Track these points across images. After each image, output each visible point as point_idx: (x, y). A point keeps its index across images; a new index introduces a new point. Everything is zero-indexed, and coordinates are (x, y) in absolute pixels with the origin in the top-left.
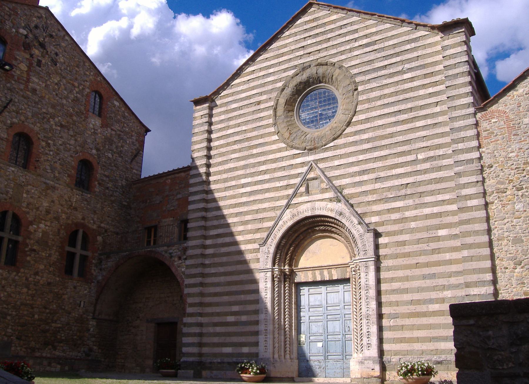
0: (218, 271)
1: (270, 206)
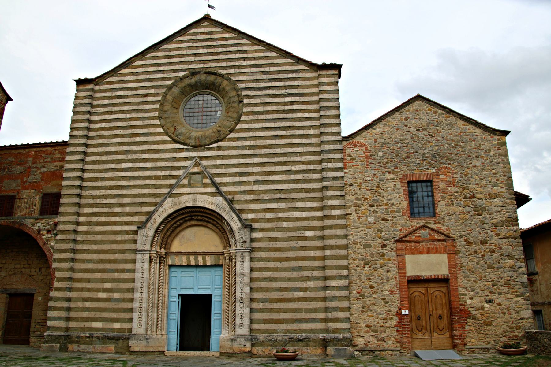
0: (90, 248)
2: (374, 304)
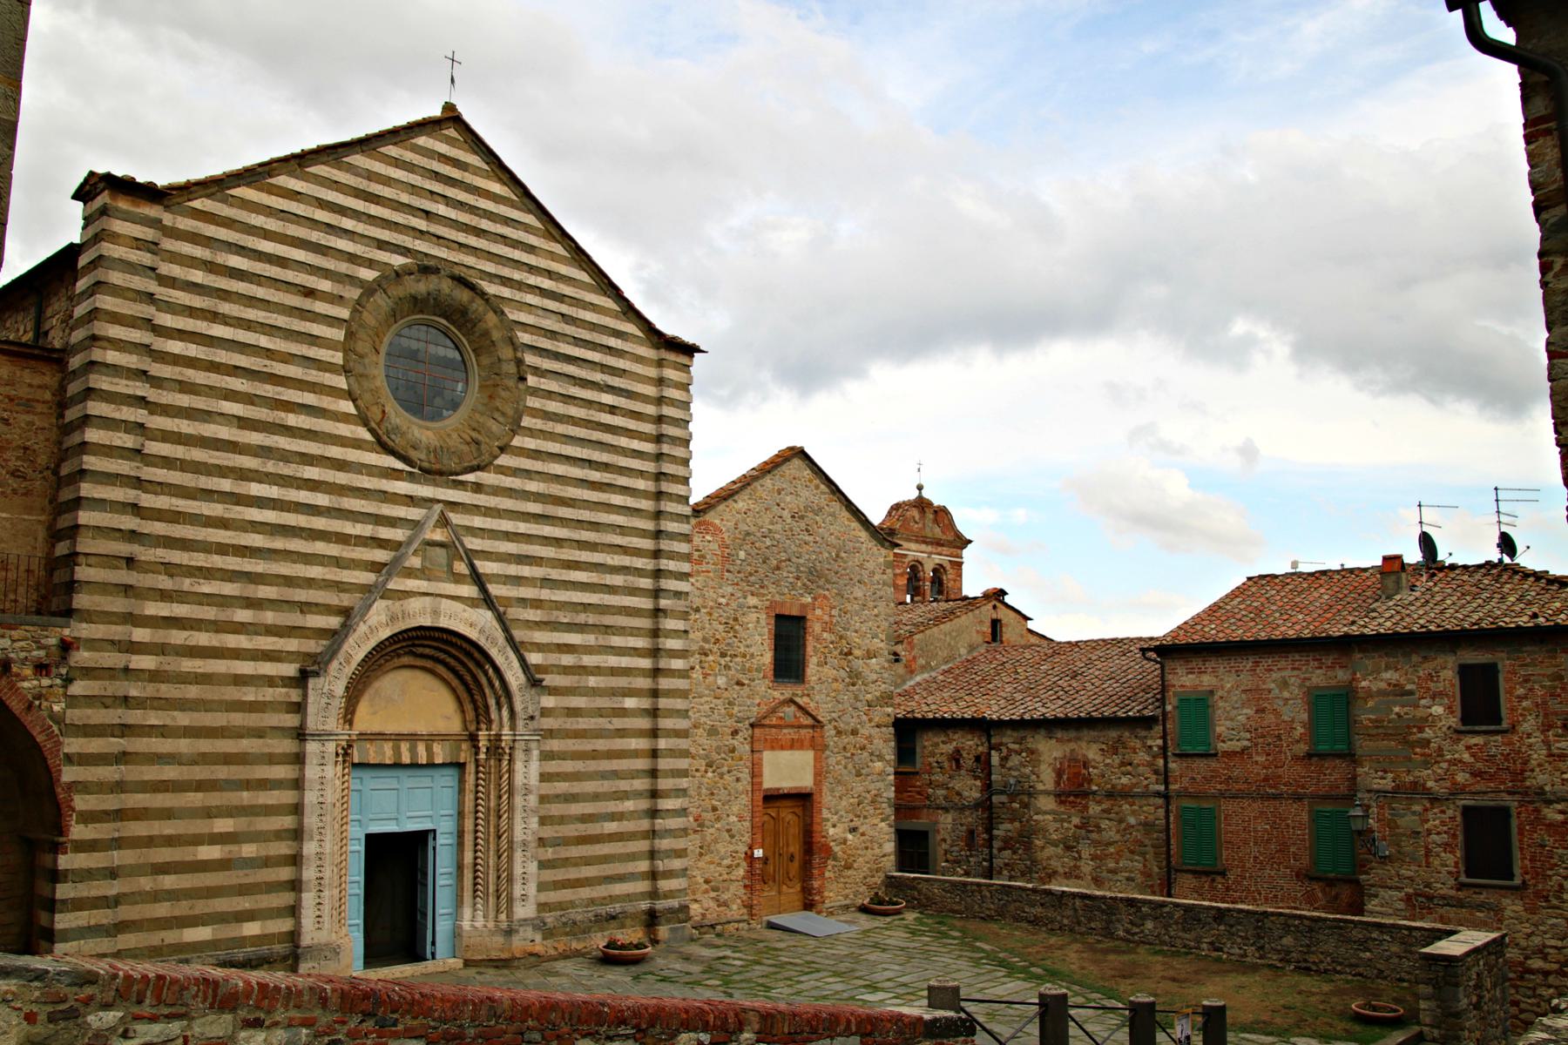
0: (169, 722)
1: (328, 577)
2: (716, 841)
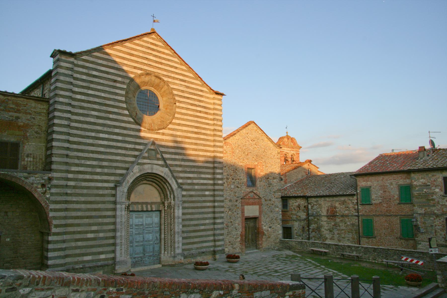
0: (79, 200)
1: (122, 159)
2: (232, 231)
